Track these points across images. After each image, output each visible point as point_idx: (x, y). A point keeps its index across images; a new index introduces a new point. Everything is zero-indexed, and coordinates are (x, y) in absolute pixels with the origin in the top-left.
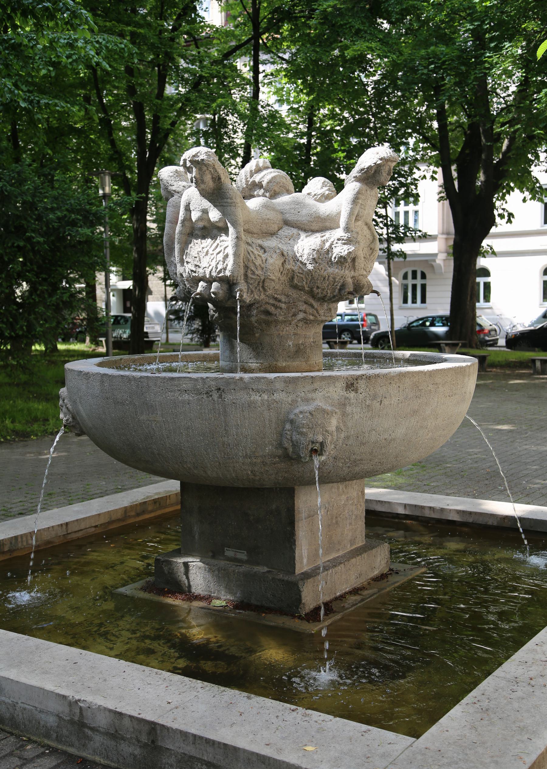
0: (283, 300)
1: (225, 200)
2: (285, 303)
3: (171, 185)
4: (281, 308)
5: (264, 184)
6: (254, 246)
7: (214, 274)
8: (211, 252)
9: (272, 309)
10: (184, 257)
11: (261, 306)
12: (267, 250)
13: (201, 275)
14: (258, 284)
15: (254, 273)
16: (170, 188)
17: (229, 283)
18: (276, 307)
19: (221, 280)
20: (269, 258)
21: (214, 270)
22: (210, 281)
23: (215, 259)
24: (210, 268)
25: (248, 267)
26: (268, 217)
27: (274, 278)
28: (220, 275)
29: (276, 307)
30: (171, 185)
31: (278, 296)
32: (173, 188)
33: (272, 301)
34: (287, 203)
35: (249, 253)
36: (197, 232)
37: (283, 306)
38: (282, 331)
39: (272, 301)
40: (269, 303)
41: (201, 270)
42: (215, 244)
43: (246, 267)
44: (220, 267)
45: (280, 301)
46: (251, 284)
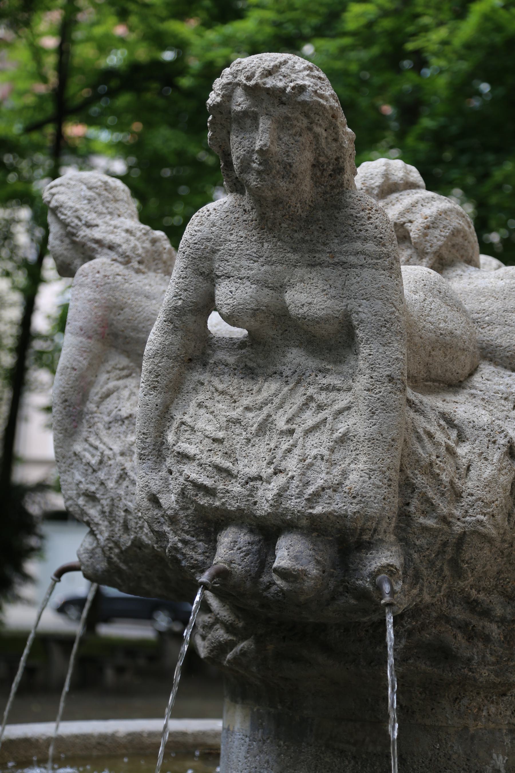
0: (499, 611)
1: (358, 245)
2: (502, 620)
3: (89, 225)
4: (487, 639)
5: (414, 231)
6: (432, 415)
7: (294, 504)
8: (281, 424)
9: (458, 642)
10: (171, 438)
11: (423, 627)
12: (468, 432)
13: (233, 506)
14: (441, 552)
15: (429, 507)
16: (84, 233)
17: (342, 540)
18: (471, 634)
19: (316, 528)
20: (478, 463)
21: (293, 491)
22: (267, 531)
23: (297, 451)
24: (280, 480)
25: (413, 488)
26: (451, 326)
27: (493, 532)
28: (318, 510)
29: (471, 634)
30: (89, 225)
31: (482, 596)
32: (97, 234)
33: (459, 613)
34: (494, 294)
35: (419, 439)
36: (221, 355)
37: (494, 630)
38: (476, 718)
39: (459, 613)
40: (448, 620)
41: (236, 488)
42: (299, 400)
43: (407, 487)
44: (319, 481)
45: (486, 613)
46: (420, 550)
